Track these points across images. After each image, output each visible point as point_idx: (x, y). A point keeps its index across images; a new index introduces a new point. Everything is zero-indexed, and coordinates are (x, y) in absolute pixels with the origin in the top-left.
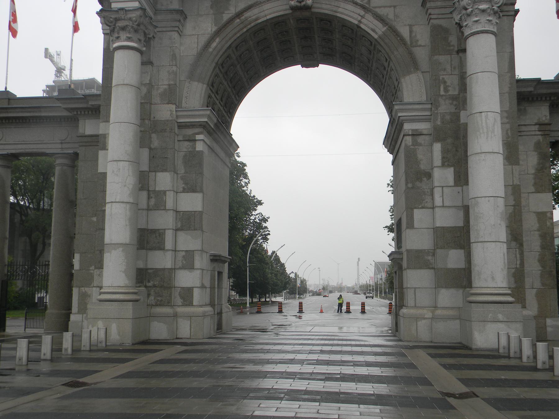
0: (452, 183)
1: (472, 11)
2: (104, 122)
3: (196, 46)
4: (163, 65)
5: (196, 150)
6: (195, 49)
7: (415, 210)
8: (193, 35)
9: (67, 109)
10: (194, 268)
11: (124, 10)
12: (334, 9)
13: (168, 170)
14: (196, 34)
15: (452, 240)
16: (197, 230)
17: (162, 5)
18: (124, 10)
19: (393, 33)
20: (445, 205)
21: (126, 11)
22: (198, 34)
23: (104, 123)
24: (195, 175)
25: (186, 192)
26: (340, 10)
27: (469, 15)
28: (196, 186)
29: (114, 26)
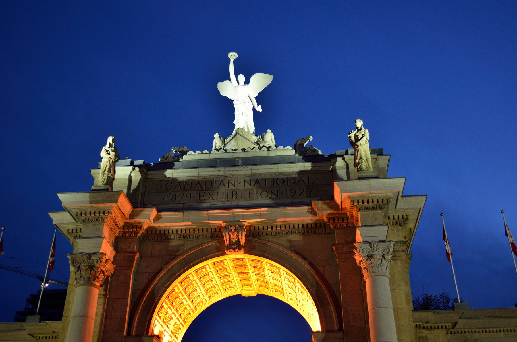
4: (117, 298)
8: (145, 273)
17: (122, 249)
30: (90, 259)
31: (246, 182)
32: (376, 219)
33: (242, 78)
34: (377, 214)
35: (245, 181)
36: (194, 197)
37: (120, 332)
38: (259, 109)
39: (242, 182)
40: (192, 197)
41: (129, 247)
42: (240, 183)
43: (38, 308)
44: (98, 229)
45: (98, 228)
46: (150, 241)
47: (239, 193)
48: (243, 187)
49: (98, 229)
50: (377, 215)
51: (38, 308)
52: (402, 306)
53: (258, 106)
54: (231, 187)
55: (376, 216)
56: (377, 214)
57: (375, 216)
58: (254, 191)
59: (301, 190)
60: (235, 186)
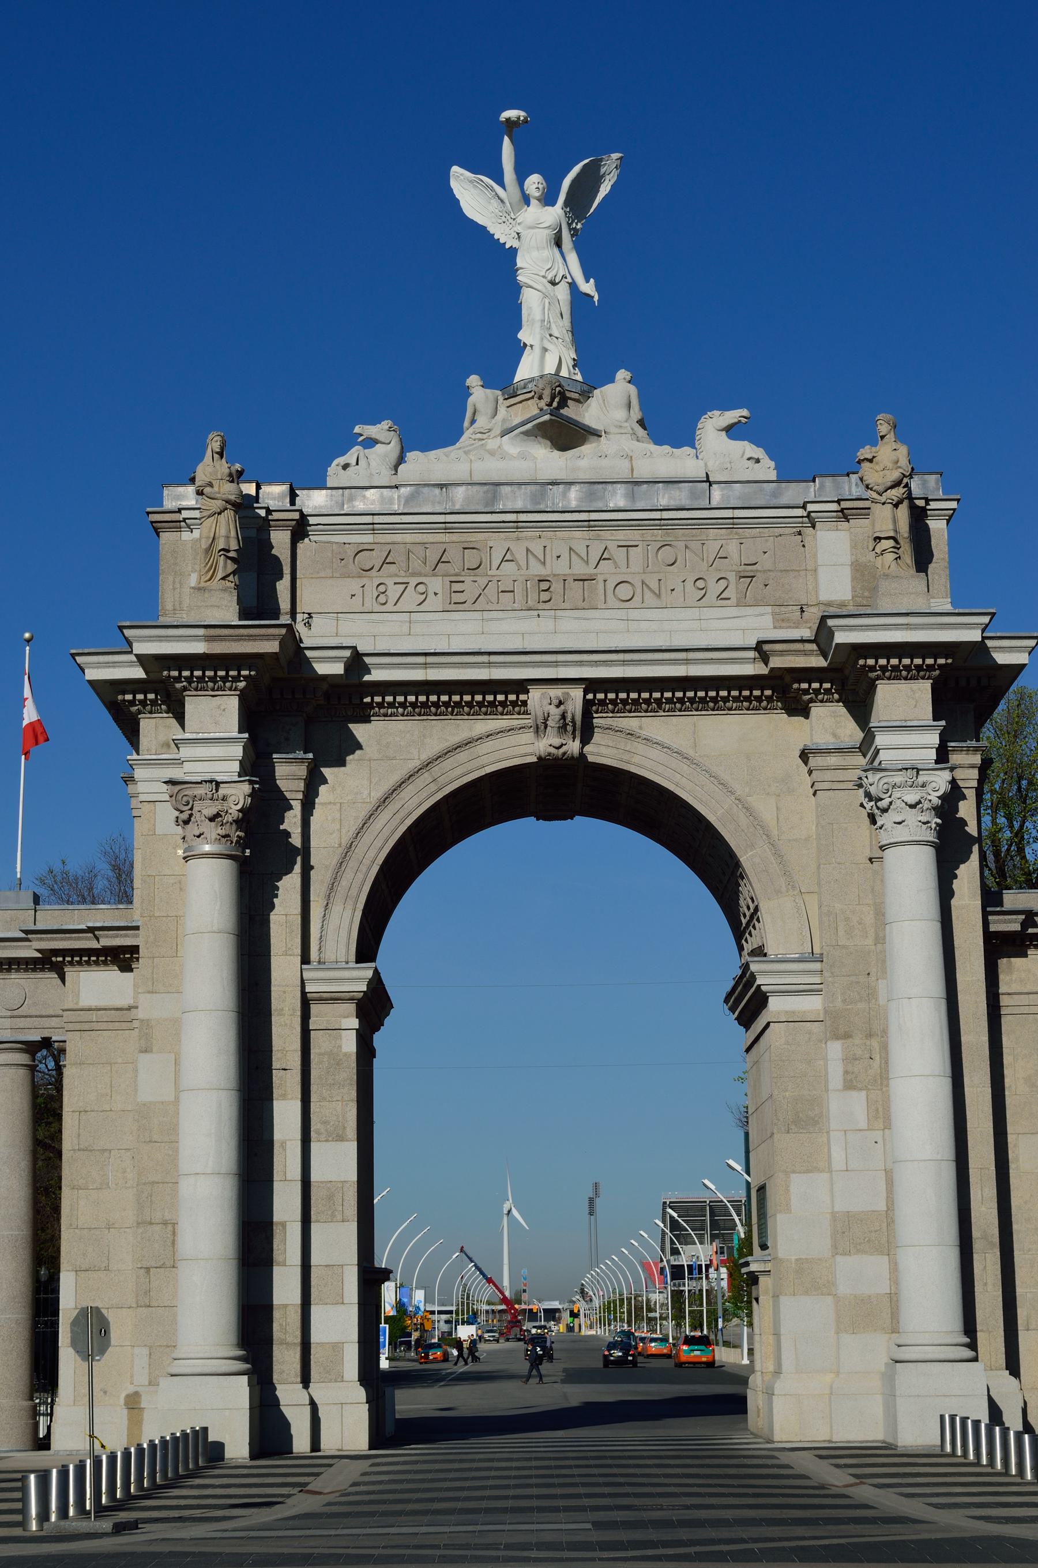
0: (863, 1124)
1: (891, 803)
2: (149, 992)
3: (338, 827)
5: (343, 1051)
6: (335, 835)
7: (793, 1176)
9: (38, 951)
10: (345, 1302)
11: (214, 783)
12: (626, 757)
13: (289, 1097)
14: (337, 800)
15: (865, 1238)
16: (348, 1221)
18: (214, 783)
19: (744, 810)
20: (849, 1169)
21: (218, 784)
22: (341, 801)
23: (148, 996)
24: (342, 1105)
25: (323, 1139)
26: (636, 759)
27: (885, 810)
28: (344, 1128)
29: (190, 812)
30: (217, 791)
31: (577, 554)
32: (917, 702)
33: (534, 183)
34: (919, 689)
35: (571, 549)
36: (436, 594)
37: (291, 955)
38: (588, 287)
39: (565, 555)
40: (431, 595)
41: (287, 739)
42: (558, 557)
43: (18, 870)
44: (224, 710)
45: (222, 708)
46: (334, 719)
47: (557, 587)
48: (567, 571)
49: (224, 710)
50: (920, 693)
51: (18, 870)
52: (960, 903)
53: (587, 281)
54: (537, 570)
55: (917, 695)
56: (919, 689)
57: (914, 694)
58: (597, 582)
59: (723, 584)
60: (544, 563)
